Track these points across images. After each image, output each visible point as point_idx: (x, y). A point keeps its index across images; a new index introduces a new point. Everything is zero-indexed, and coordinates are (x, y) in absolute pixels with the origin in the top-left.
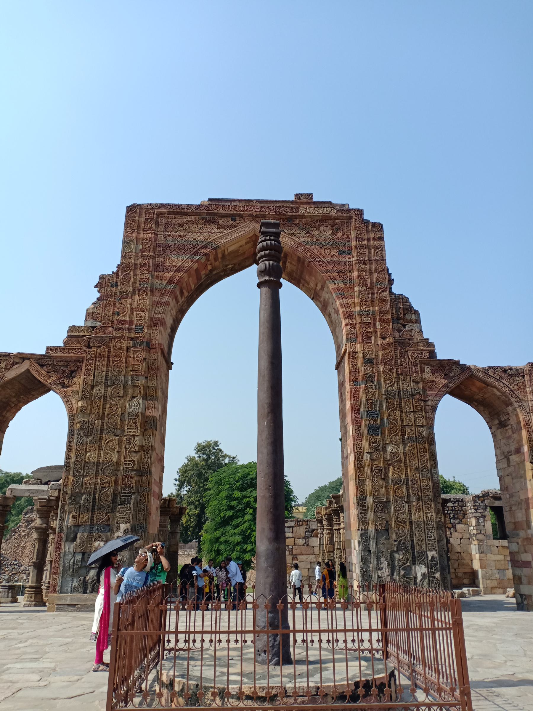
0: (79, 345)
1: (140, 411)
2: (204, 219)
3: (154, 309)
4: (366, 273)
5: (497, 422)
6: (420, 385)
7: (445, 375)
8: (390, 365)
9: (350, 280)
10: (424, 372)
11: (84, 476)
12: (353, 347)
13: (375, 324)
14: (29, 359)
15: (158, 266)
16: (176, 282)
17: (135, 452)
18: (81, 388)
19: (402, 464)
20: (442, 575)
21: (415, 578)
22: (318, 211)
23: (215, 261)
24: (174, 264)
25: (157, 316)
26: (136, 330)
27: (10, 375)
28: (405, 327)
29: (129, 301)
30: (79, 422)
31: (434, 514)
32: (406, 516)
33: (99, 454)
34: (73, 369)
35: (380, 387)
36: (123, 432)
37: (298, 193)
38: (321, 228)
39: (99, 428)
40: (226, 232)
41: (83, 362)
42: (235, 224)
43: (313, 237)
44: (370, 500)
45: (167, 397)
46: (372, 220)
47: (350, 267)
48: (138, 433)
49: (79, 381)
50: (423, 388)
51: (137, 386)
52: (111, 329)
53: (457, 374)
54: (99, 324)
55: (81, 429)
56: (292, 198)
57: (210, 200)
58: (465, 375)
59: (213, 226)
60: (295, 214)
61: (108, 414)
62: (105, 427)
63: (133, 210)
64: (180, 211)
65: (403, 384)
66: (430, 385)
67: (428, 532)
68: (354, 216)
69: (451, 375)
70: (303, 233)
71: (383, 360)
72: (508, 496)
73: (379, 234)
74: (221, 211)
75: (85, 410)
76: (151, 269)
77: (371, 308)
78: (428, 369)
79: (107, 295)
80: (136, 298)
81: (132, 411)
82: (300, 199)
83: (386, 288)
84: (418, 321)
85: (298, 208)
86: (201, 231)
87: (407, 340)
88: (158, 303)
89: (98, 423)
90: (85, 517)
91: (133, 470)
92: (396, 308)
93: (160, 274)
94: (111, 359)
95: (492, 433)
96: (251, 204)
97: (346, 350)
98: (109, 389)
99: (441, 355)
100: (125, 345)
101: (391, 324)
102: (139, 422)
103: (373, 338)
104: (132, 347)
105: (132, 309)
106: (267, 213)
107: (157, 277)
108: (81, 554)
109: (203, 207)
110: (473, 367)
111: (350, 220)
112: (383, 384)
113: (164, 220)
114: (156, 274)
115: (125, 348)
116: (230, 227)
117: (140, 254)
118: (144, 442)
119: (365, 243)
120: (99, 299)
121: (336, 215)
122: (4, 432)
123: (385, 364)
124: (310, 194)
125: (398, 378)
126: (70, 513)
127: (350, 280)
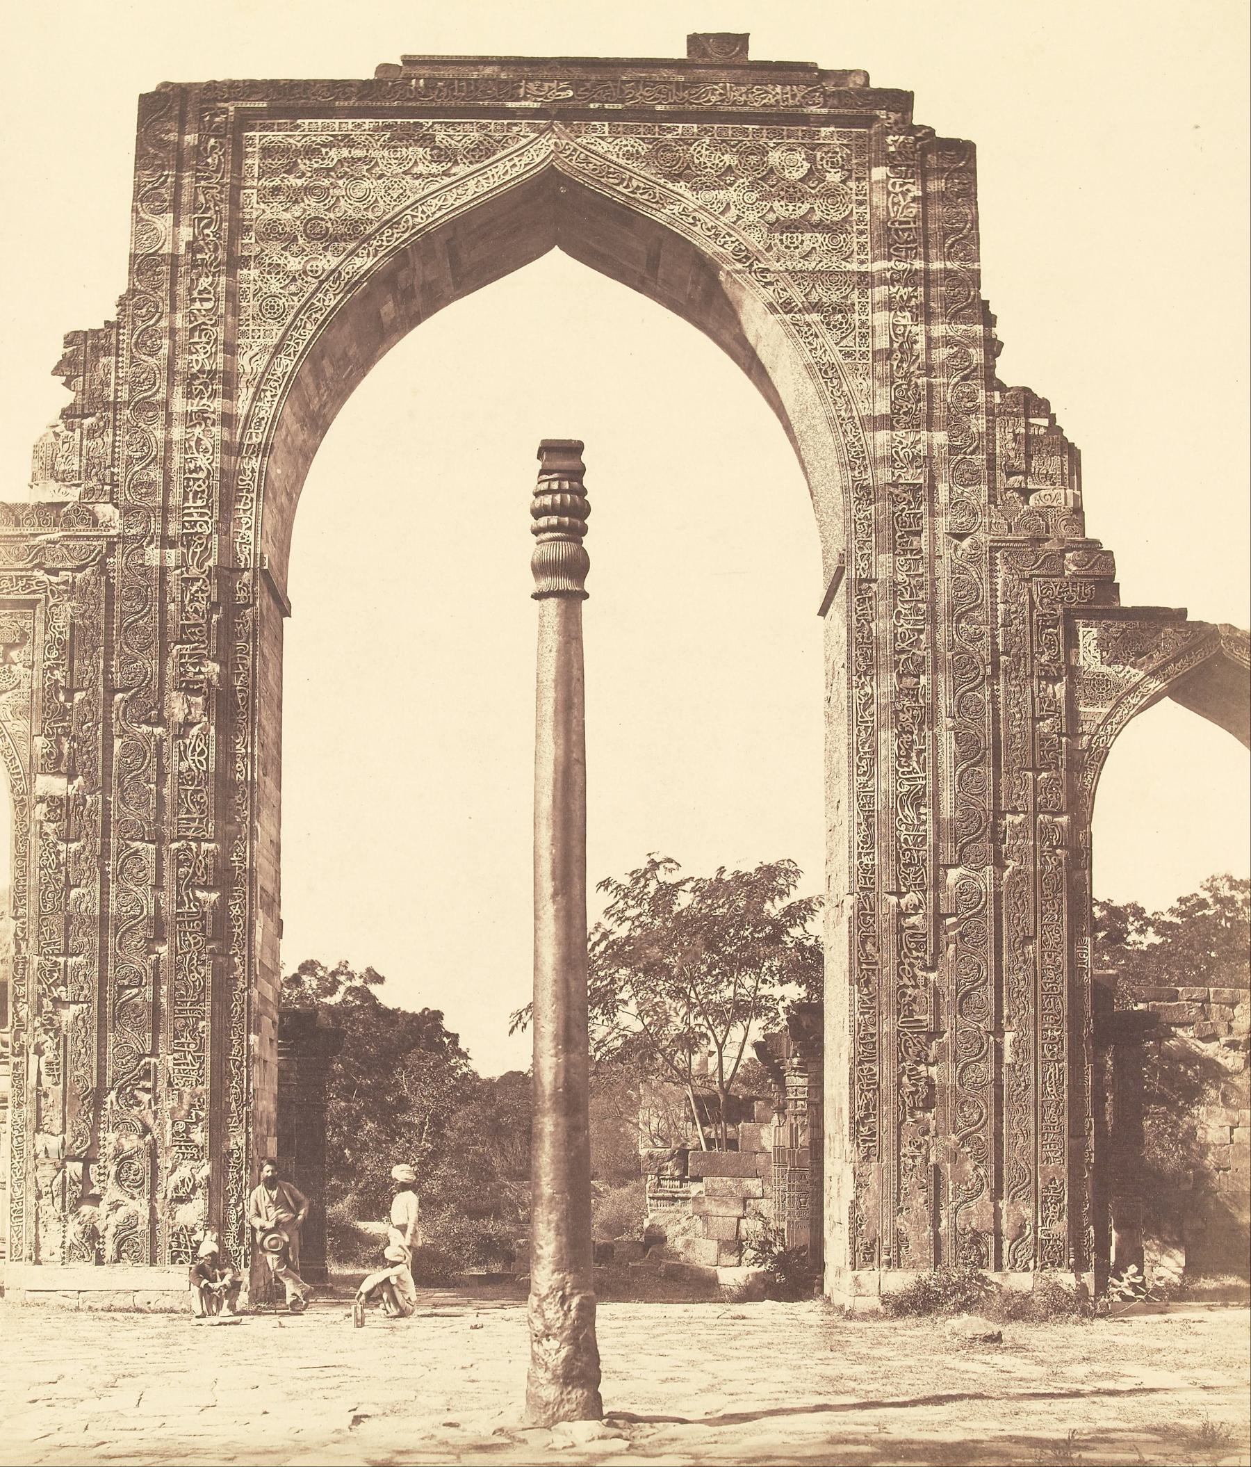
8: (972, 621)
10: (1077, 646)
16: (301, 348)
19: (989, 925)
30: (42, 800)
33: (104, 893)
40: (461, 170)
54: (73, 495)
57: (409, 61)
76: (222, 310)
78: (1088, 635)
81: (190, 769)
82: (704, 54)
83: (975, 370)
94: (117, 607)
100: (156, 562)
104: (177, 568)
106: (592, 106)
113: (256, 137)
120: (68, 414)
125: (995, 664)
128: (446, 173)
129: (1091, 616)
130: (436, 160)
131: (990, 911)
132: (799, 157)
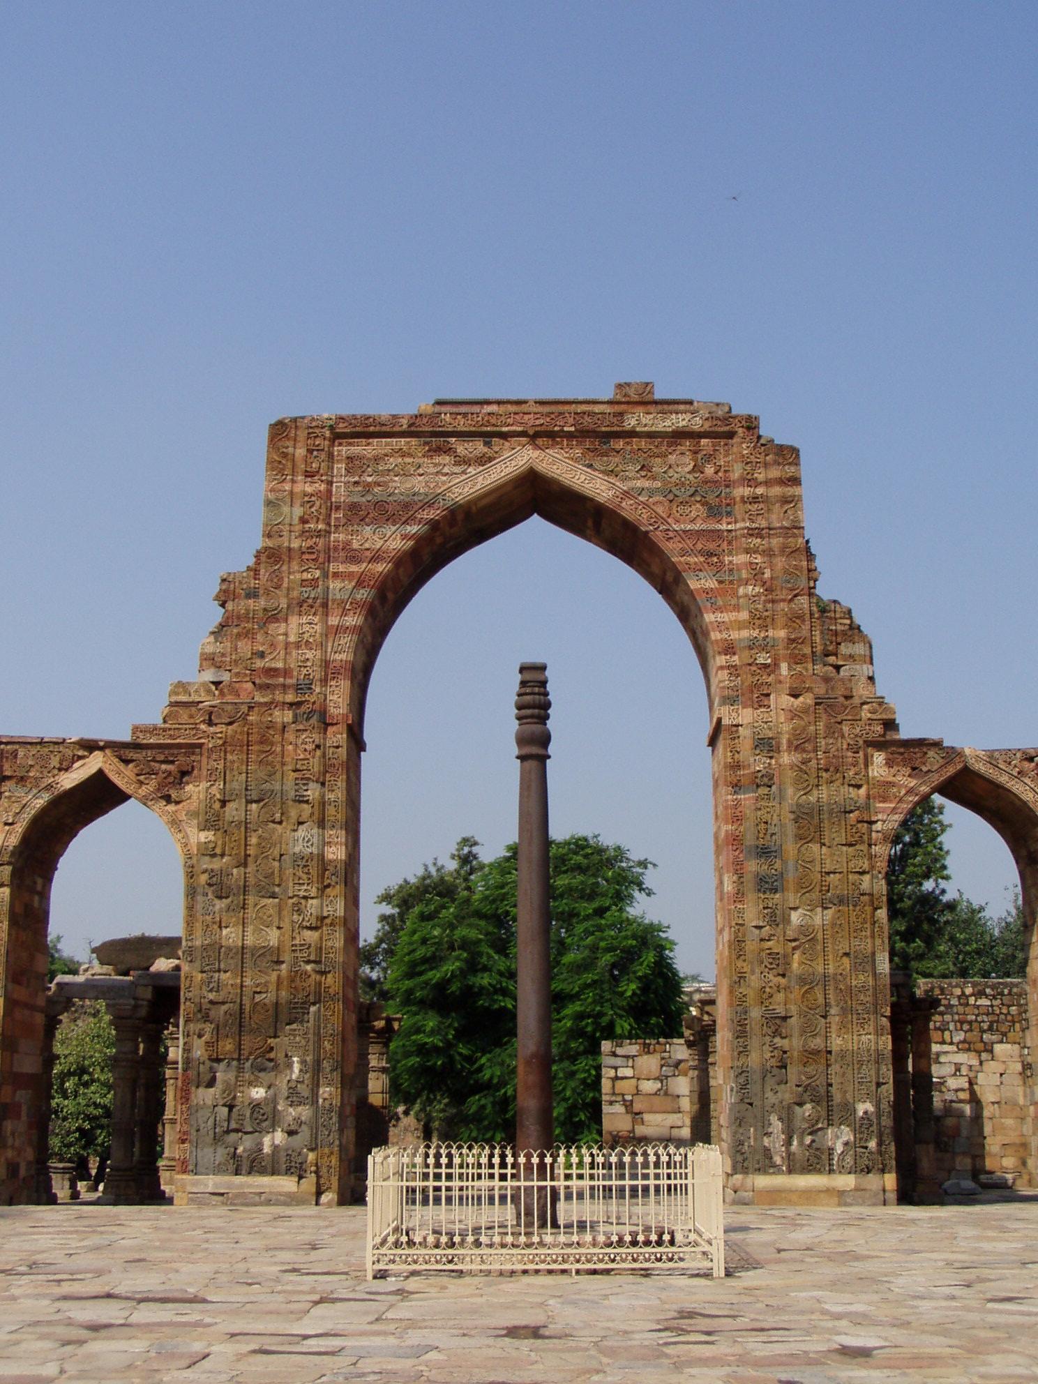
0: (192, 721)
1: (315, 852)
2: (426, 443)
3: (330, 644)
5: (1024, 853)
6: (863, 791)
7: (914, 769)
8: (804, 751)
9: (731, 570)
11: (219, 971)
13: (776, 665)
14: (101, 749)
15: (336, 549)
17: (307, 928)
18: (202, 806)
19: (819, 947)
20: (880, 1144)
21: (831, 1150)
22: (663, 420)
23: (451, 526)
24: (367, 545)
25: (338, 657)
26: (298, 688)
27: (68, 781)
28: (838, 672)
29: (283, 625)
30: (205, 872)
32: (817, 1043)
34: (185, 769)
35: (782, 798)
36: (285, 891)
37: (622, 381)
39: (242, 883)
40: (472, 470)
41: (201, 754)
42: (490, 453)
43: (654, 478)
44: (756, 1013)
45: (359, 811)
47: (730, 543)
48: (313, 892)
49: (196, 791)
50: (868, 797)
51: (307, 802)
52: (250, 685)
53: (935, 768)
55: (210, 885)
56: (608, 394)
57: (439, 403)
58: (951, 770)
59: (446, 459)
60: (615, 429)
61: (256, 857)
62: (252, 881)
63: (280, 431)
64: (378, 429)
65: (828, 788)
66: (884, 790)
67: (859, 1069)
68: (740, 430)
69: (925, 769)
70: (632, 469)
71: (790, 742)
73: (790, 471)
74: (462, 425)
75: (214, 848)
76: (321, 560)
77: (770, 633)
79: (238, 618)
80: (294, 620)
85: (621, 414)
86: (420, 471)
87: (842, 699)
88: (338, 630)
89: (239, 873)
90: (228, 1046)
91: (308, 962)
92: (822, 633)
93: (342, 568)
95: (1020, 872)
96: (524, 408)
97: (719, 720)
98: (254, 806)
101: (810, 666)
102: (314, 872)
103: (772, 697)
105: (287, 645)
107: (336, 575)
108: (226, 1109)
109: (425, 420)
110: (967, 751)
111: (731, 438)
112: (790, 791)
113: (342, 450)
114: (333, 567)
115: (279, 726)
116: (483, 460)
117: (298, 528)
118: (325, 909)
119: (760, 491)
120: (222, 626)
122: (51, 880)
123: (797, 748)
124: (647, 384)
126: (200, 1036)
128: (464, 472)
129: (879, 745)
130: (457, 464)
131: (820, 936)
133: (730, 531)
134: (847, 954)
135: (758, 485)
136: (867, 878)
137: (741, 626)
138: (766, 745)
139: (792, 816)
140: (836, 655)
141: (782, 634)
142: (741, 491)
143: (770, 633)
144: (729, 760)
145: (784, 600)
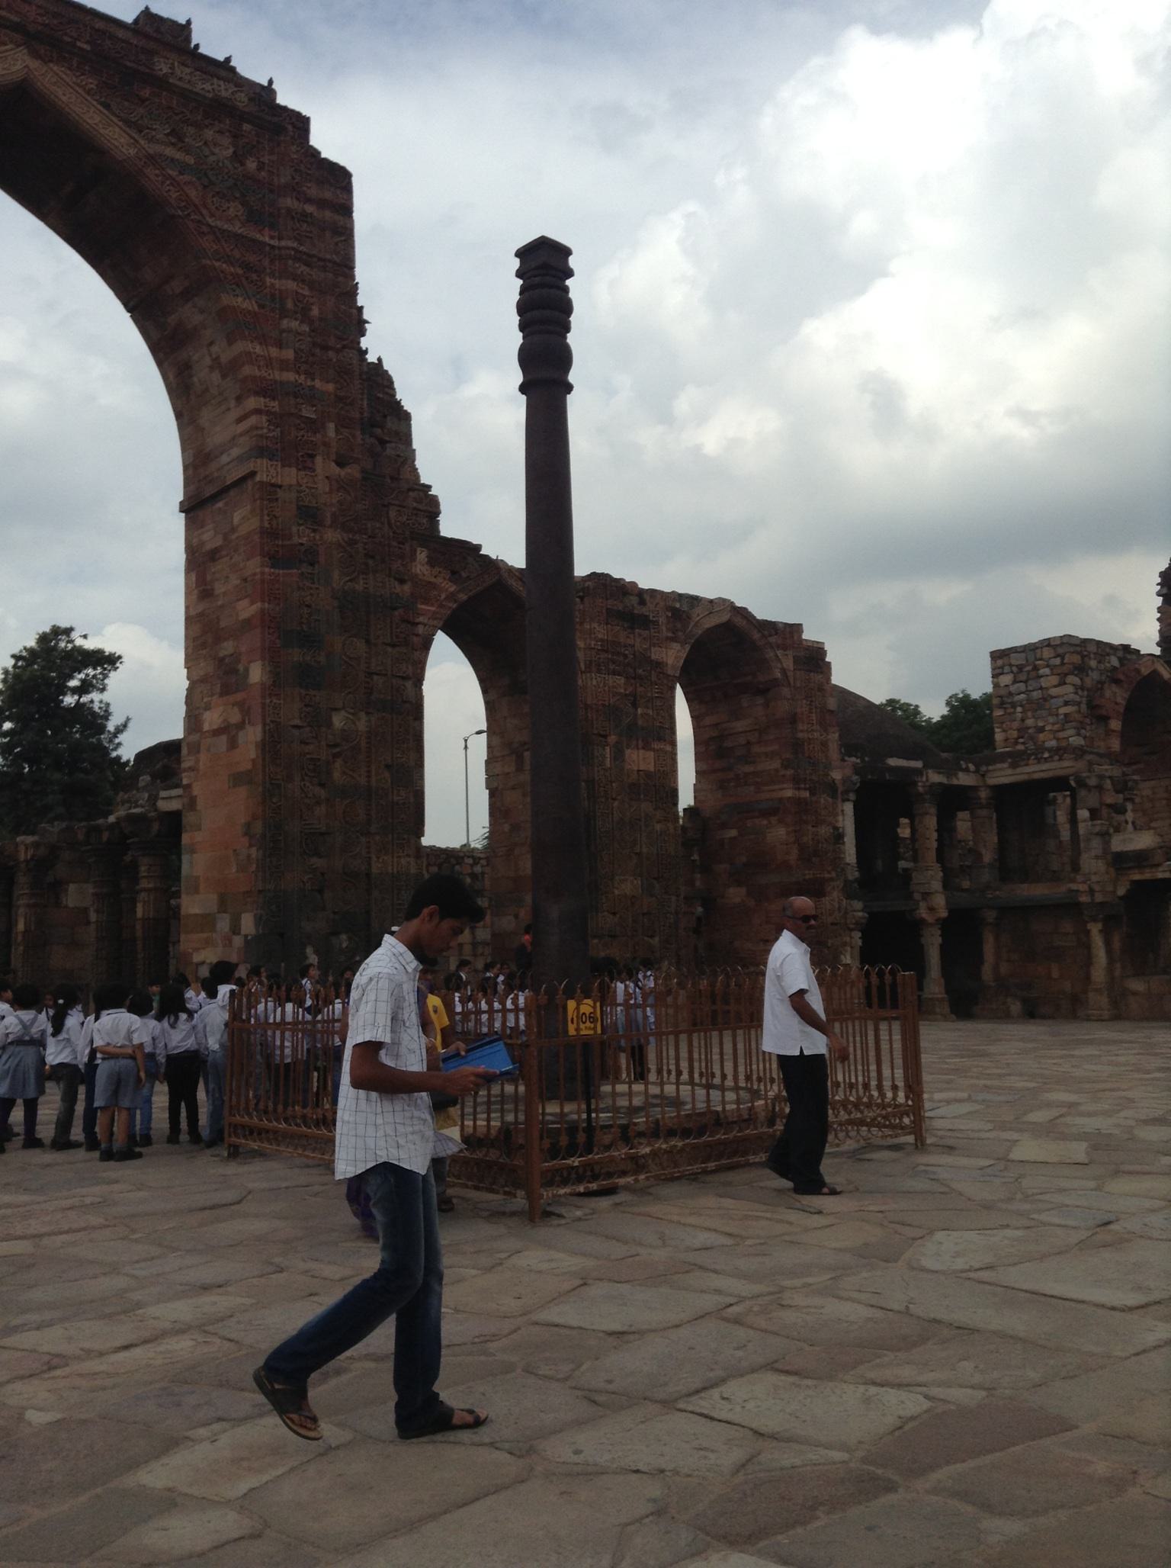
4: (311, 289)
6: (407, 588)
7: (454, 573)
10: (415, 560)
12: (272, 471)
31: (412, 860)
38: (209, 134)
46: (329, 152)
47: (272, 261)
68: (290, 128)
69: (464, 575)
72: (506, 827)
78: (422, 555)
84: (406, 438)
95: (487, 703)
99: (449, 527)
103: (319, 460)
112: (336, 575)
119: (310, 208)
121: (246, 110)
127: (273, 296)
131: (363, 744)
132: (226, 141)
133: (273, 247)
134: (387, 766)
135: (309, 200)
136: (409, 684)
137: (284, 366)
138: (309, 515)
139: (336, 603)
140: (382, 427)
141: (330, 387)
142: (289, 202)
143: (318, 384)
144: (266, 525)
145: (331, 348)
